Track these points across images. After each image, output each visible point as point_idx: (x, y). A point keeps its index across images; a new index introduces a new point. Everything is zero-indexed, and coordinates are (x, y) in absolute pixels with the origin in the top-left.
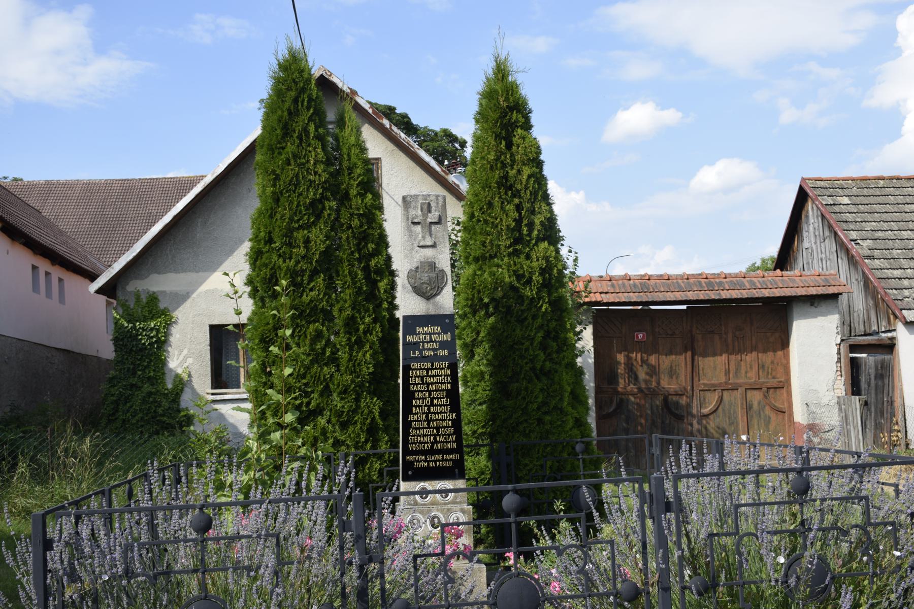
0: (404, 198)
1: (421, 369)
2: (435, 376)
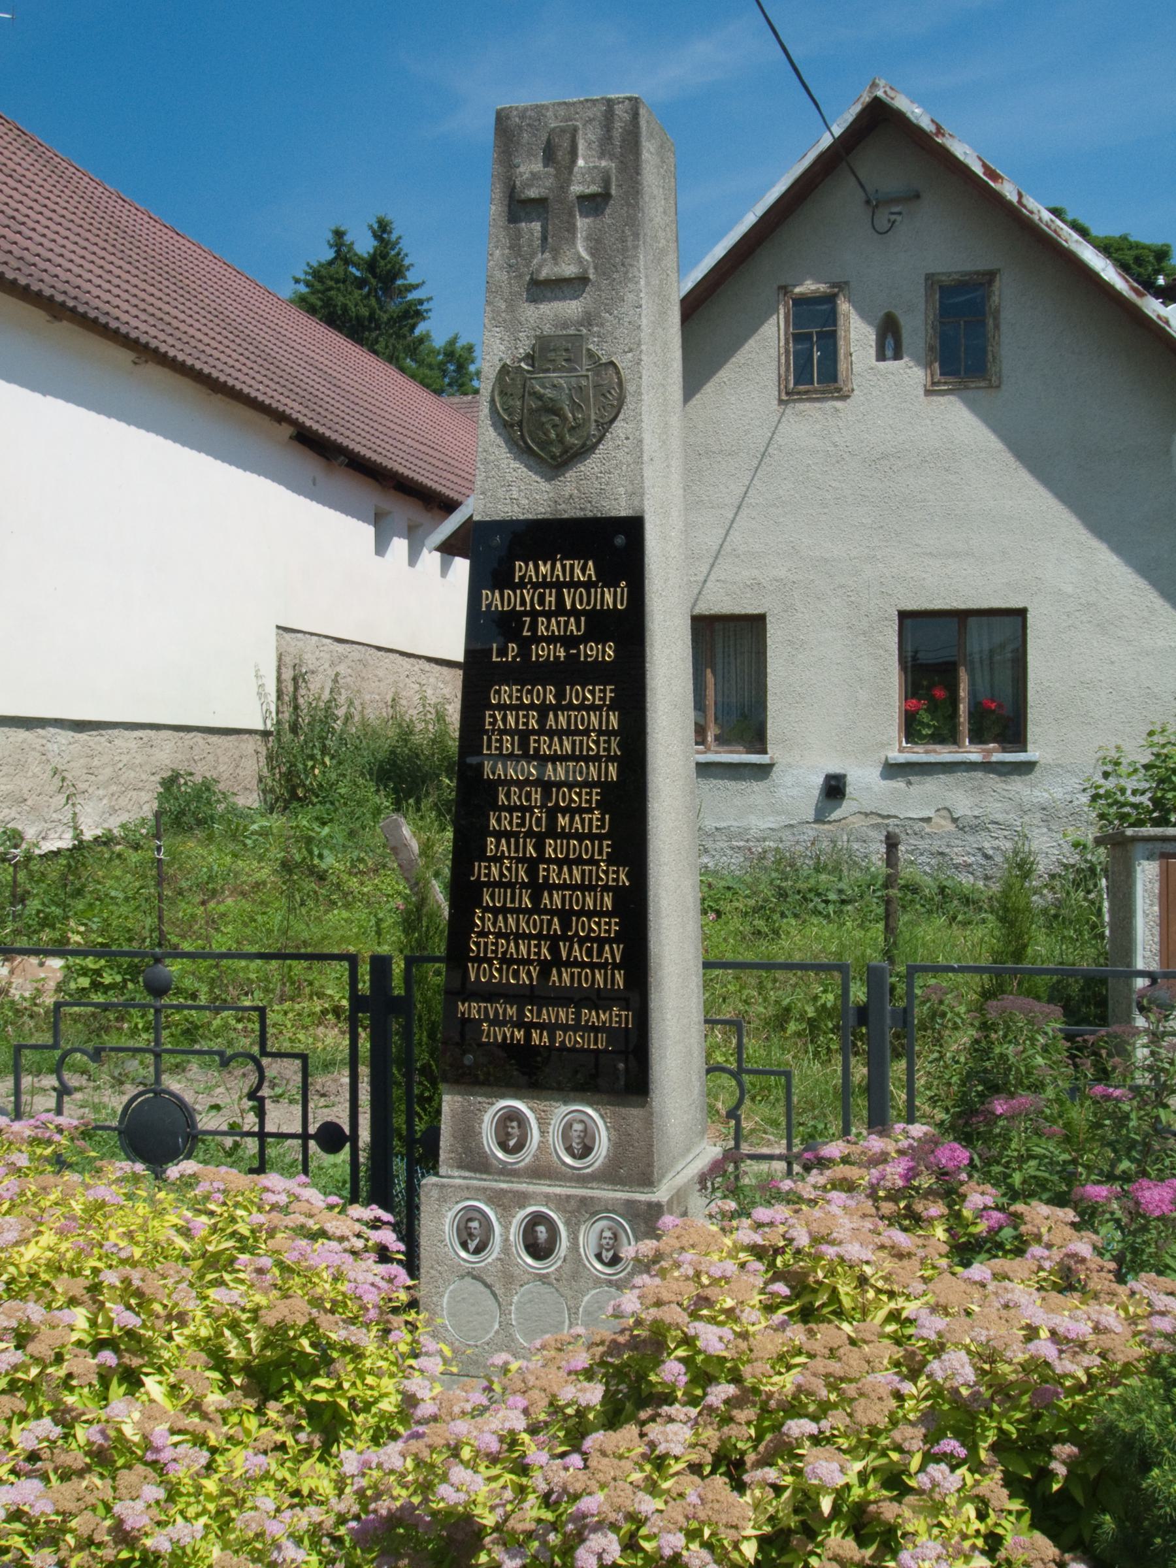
0: (502, 118)
1: (522, 707)
2: (568, 732)
